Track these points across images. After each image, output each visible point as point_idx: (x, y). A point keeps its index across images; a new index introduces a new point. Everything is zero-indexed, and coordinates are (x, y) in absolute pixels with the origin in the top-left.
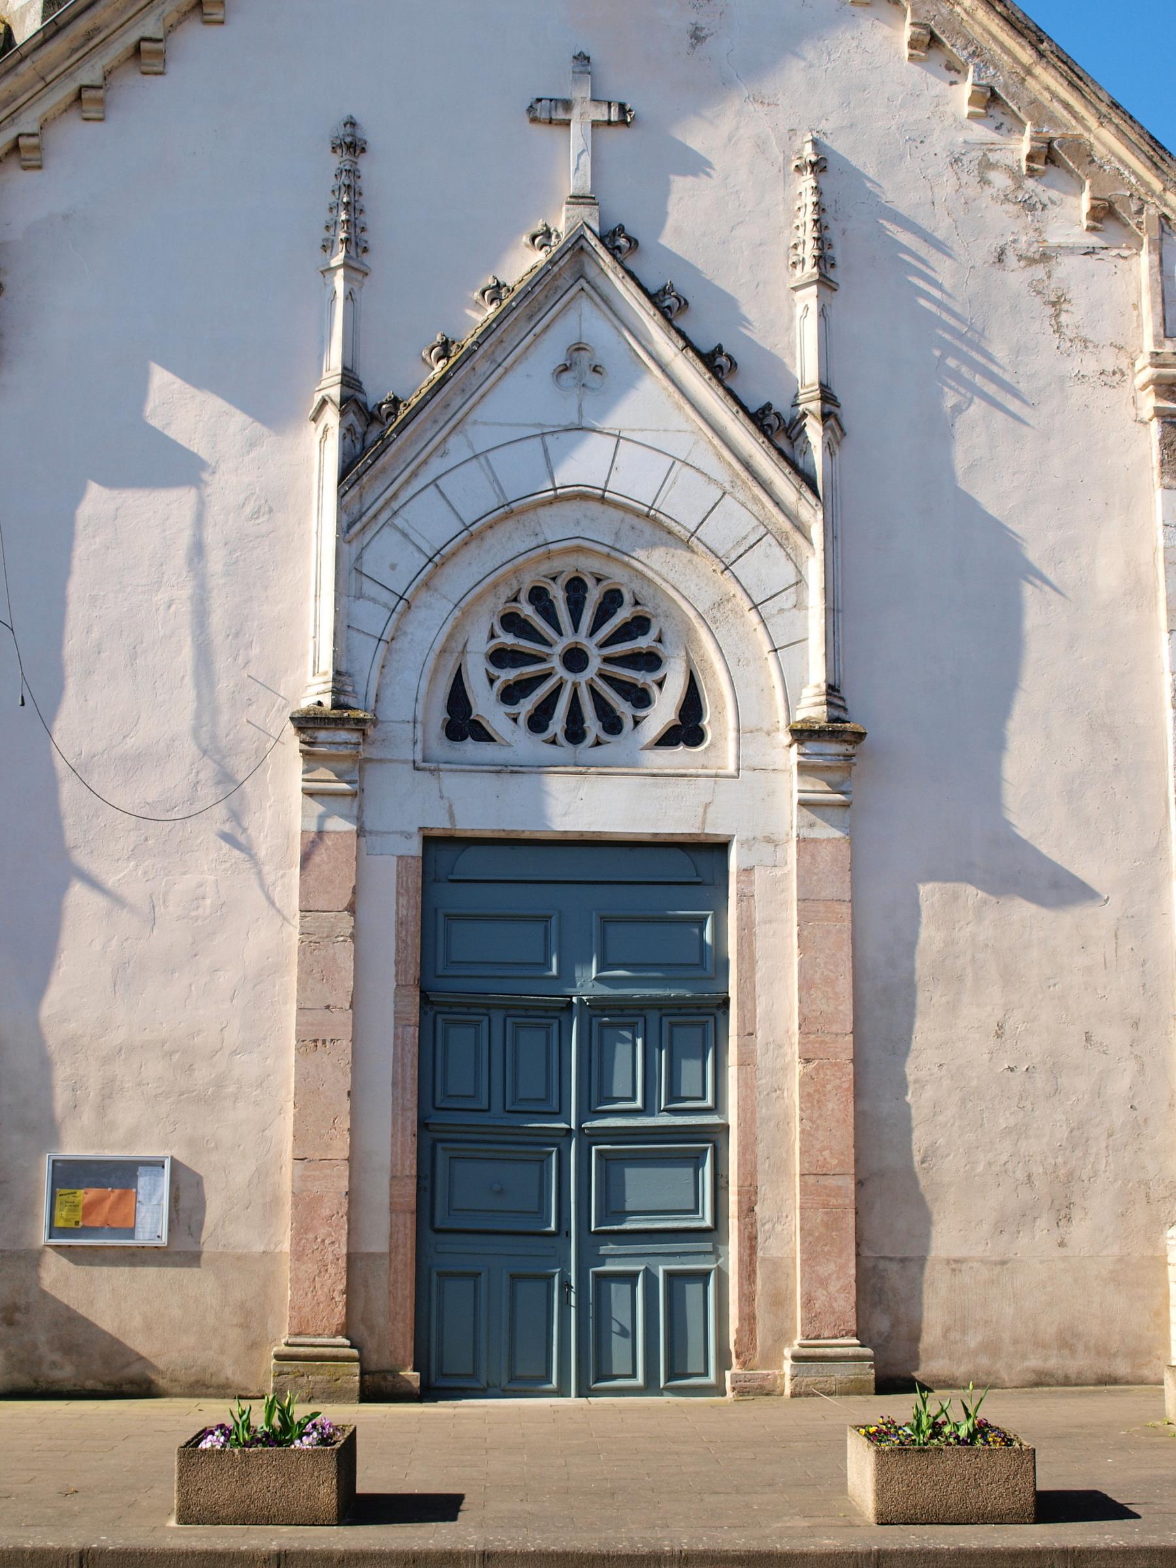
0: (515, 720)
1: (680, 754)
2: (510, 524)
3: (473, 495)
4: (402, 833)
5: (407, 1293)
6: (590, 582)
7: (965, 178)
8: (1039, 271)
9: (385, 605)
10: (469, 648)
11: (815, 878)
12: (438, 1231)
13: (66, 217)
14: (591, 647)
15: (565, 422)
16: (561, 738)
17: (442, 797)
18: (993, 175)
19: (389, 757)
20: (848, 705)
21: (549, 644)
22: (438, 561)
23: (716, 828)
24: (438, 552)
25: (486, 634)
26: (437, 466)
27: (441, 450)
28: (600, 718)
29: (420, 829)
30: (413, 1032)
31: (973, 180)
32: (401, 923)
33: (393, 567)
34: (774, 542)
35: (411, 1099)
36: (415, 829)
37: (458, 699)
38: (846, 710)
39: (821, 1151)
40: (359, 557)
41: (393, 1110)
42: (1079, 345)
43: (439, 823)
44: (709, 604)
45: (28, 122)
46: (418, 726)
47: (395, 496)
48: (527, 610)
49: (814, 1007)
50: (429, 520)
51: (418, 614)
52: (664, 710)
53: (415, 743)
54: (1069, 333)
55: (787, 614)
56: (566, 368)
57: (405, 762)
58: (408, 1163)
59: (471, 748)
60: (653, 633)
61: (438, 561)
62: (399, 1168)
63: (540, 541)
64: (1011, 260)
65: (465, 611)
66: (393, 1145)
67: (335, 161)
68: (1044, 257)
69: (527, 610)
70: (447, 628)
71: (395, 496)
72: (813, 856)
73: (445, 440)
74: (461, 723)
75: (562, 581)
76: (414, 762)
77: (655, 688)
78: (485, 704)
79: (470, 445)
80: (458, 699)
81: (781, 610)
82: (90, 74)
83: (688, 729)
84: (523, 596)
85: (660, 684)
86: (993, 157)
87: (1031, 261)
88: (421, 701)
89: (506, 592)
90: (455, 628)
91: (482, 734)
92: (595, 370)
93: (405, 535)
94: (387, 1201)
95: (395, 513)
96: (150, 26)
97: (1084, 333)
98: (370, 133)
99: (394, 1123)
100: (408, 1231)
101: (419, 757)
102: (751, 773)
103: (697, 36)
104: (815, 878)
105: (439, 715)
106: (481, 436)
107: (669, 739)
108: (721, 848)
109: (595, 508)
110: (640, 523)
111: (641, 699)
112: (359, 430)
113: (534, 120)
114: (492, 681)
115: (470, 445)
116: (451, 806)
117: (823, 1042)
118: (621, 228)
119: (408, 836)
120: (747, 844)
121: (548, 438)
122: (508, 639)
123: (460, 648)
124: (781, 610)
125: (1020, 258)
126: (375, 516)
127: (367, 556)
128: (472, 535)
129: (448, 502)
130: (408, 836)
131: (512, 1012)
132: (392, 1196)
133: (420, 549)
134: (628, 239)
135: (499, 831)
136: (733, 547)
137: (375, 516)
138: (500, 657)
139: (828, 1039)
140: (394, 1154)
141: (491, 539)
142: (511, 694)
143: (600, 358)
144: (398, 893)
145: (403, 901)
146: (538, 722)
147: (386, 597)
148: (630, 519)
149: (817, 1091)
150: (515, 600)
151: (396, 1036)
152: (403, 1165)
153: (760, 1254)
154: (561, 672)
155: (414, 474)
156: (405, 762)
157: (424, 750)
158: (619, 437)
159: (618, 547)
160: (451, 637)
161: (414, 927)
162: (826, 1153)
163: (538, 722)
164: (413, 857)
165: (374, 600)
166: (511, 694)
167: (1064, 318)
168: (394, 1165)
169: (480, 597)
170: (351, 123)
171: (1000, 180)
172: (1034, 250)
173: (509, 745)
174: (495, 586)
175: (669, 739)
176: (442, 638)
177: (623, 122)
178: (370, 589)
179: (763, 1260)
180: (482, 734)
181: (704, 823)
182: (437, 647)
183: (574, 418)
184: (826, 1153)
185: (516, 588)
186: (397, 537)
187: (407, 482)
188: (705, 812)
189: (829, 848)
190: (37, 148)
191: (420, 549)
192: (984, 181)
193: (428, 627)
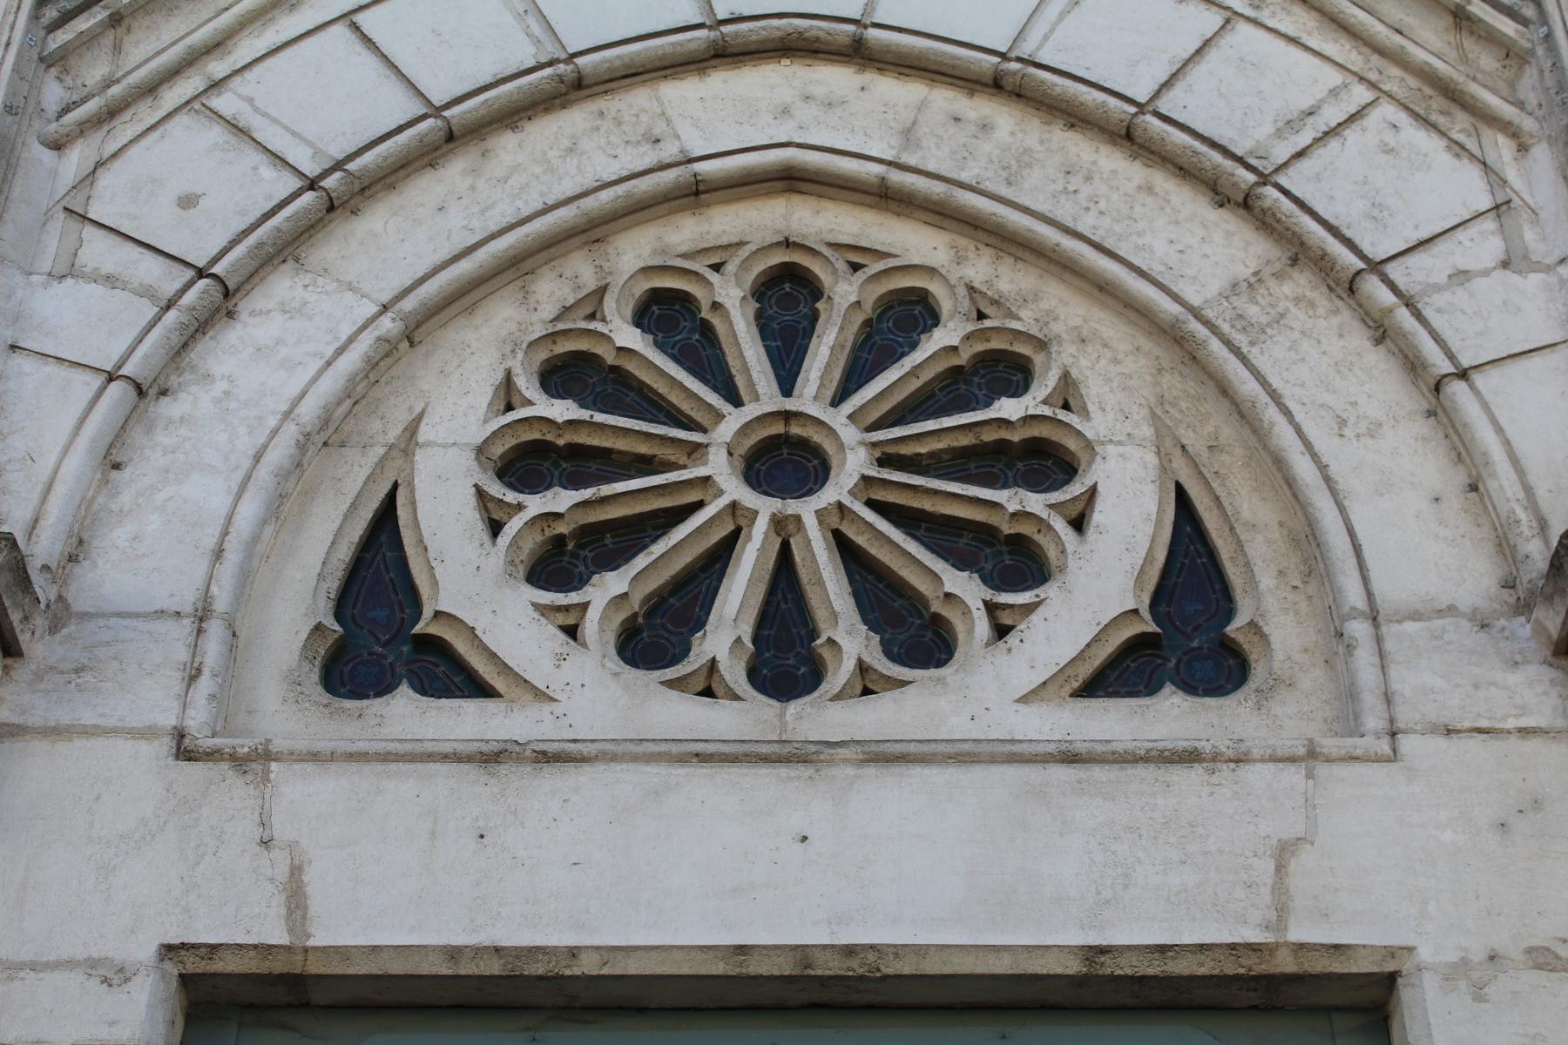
0: (572, 631)
1: (1170, 715)
9: (147, 292)
10: (425, 433)
16: (734, 673)
17: (266, 843)
19: (88, 718)
22: (340, 195)
24: (338, 166)
25: (483, 393)
29: (169, 950)
34: (1402, 118)
36: (145, 951)
44: (1214, 287)
46: (215, 629)
47: (216, 46)
52: (1102, 580)
53: (194, 676)
55: (1479, 283)
57: (147, 733)
59: (405, 714)
61: (340, 195)
63: (669, 151)
65: (420, 325)
70: (351, 361)
74: (382, 635)
76: (180, 734)
78: (469, 579)
81: (1461, 276)
85: (1079, 524)
88: (233, 557)
89: (552, 291)
91: (447, 671)
95: (216, 85)
102: (1441, 742)
105: (296, 603)
107: (1123, 671)
109: (835, 78)
111: (1017, 563)
114: (495, 528)
116: (296, 871)
120: (1477, 974)
123: (394, 433)
126: (151, 89)
127: (105, 180)
129: (384, 57)
130: (115, 975)
135: (478, 951)
136: (1279, 134)
138: (527, 462)
141: (508, 147)
142: (558, 564)
146: (655, 638)
148: (944, 99)
156: (147, 733)
159: (912, 160)
165: (111, 281)
173: (542, 696)
174: (518, 267)
175: (1123, 671)
176: (331, 384)
178: (98, 251)
180: (447, 671)
181: (1282, 910)
182: (309, 410)
185: (590, 282)
188: (1280, 868)
191: (279, 160)
193: (290, 346)
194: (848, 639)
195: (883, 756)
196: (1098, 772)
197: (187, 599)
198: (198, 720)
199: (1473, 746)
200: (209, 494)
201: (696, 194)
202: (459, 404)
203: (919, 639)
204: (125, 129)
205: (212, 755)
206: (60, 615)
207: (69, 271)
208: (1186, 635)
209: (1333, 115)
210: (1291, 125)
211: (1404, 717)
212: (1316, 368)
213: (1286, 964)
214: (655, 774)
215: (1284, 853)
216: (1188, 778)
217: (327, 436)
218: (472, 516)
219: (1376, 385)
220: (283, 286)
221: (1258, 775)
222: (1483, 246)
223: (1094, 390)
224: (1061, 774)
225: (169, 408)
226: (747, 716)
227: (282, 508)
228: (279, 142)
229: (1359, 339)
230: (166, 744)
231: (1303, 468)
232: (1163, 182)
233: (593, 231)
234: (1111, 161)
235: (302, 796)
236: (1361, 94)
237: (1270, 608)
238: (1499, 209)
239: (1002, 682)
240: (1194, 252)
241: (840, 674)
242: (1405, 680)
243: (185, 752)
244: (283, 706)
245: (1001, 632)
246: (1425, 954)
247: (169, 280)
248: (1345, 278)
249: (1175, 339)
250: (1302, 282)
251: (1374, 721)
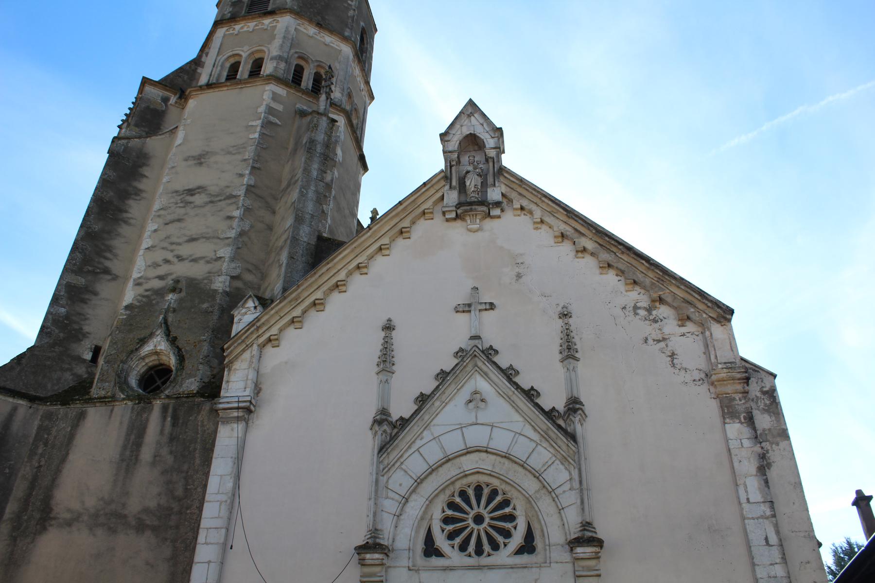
1: (525, 558)
2: (449, 464)
3: (434, 454)
6: (484, 486)
7: (627, 313)
8: (662, 344)
13: (286, 363)
14: (485, 513)
15: (470, 422)
16: (473, 554)
18: (639, 311)
20: (597, 531)
21: (467, 514)
22: (419, 481)
25: (440, 511)
26: (419, 443)
27: (420, 436)
28: (490, 544)
31: (632, 313)
33: (401, 485)
37: (429, 539)
38: (596, 533)
40: (387, 482)
42: (684, 371)
45: (274, 331)
47: (401, 456)
48: (458, 500)
50: (416, 465)
51: (411, 504)
52: (518, 539)
54: (678, 366)
56: (470, 401)
59: (435, 561)
60: (512, 506)
61: (419, 481)
63: (462, 470)
64: (650, 341)
65: (431, 501)
67: (383, 334)
68: (664, 339)
69: (458, 500)
70: (423, 509)
71: (401, 456)
73: (422, 432)
74: (431, 550)
75: (473, 487)
77: (513, 529)
78: (441, 541)
79: (432, 434)
80: (429, 539)
81: (564, 492)
82: (297, 312)
83: (528, 547)
84: (456, 494)
85: (515, 528)
86: (639, 305)
87: (659, 341)
89: (448, 492)
90: (426, 508)
91: (439, 554)
92: (482, 400)
93: (406, 472)
95: (402, 463)
96: (319, 295)
97: (684, 366)
98: (396, 322)
101: (410, 565)
103: (519, 276)
105: (420, 546)
106: (437, 431)
107: (520, 551)
109: (484, 455)
110: (504, 460)
111: (507, 534)
112: (389, 431)
113: (457, 312)
114: (443, 531)
115: (432, 434)
118: (491, 346)
121: (464, 429)
122: (450, 512)
124: (564, 492)
125: (654, 340)
126: (394, 465)
127: (390, 481)
128: (433, 470)
133: (412, 477)
134: (494, 350)
137: (394, 465)
138: (447, 520)
142: (451, 536)
143: (484, 396)
146: (463, 547)
147: (397, 497)
148: (499, 458)
150: (453, 496)
154: (472, 525)
155: (409, 447)
157: (413, 562)
158: (492, 426)
160: (425, 512)
163: (463, 547)
165: (393, 499)
166: (451, 536)
167: (675, 361)
169: (437, 495)
170: (389, 320)
171: (642, 313)
172: (660, 337)
174: (444, 490)
175: (520, 551)
177: (492, 309)
178: (391, 494)
180: (439, 554)
182: (419, 517)
183: (474, 420)
186: (403, 473)
187: (406, 450)
190: (277, 339)
191: (412, 477)
192: (636, 314)
194: (487, 547)
195: (491, 567)
196: (515, 570)
197: (407, 548)
198: (410, 565)
199: (559, 565)
200: (407, 531)
201: (466, 476)
202: (437, 513)
203: (495, 546)
204: (391, 472)
206: (393, 550)
207: (387, 498)
208: (528, 547)
209: (550, 463)
210: (544, 465)
212: (545, 505)
214: (463, 572)
216: (526, 570)
217: (422, 519)
218: (440, 531)
219: (552, 509)
220: (414, 496)
221: (534, 570)
222: (567, 487)
223: (518, 507)
224: (511, 570)
225: (402, 517)
226: (473, 561)
227: (417, 532)
228: (411, 474)
229: (551, 500)
231: (543, 522)
232: (527, 473)
233: (453, 483)
234: (520, 469)
235: (424, 575)
236: (554, 458)
237: (538, 542)
238: (570, 479)
239: (504, 556)
240: (530, 485)
241: (485, 554)
242: (553, 555)
243: (410, 570)
244: (420, 560)
245: (505, 545)
247: (400, 499)
248: (551, 492)
249: (529, 500)
250: (544, 491)
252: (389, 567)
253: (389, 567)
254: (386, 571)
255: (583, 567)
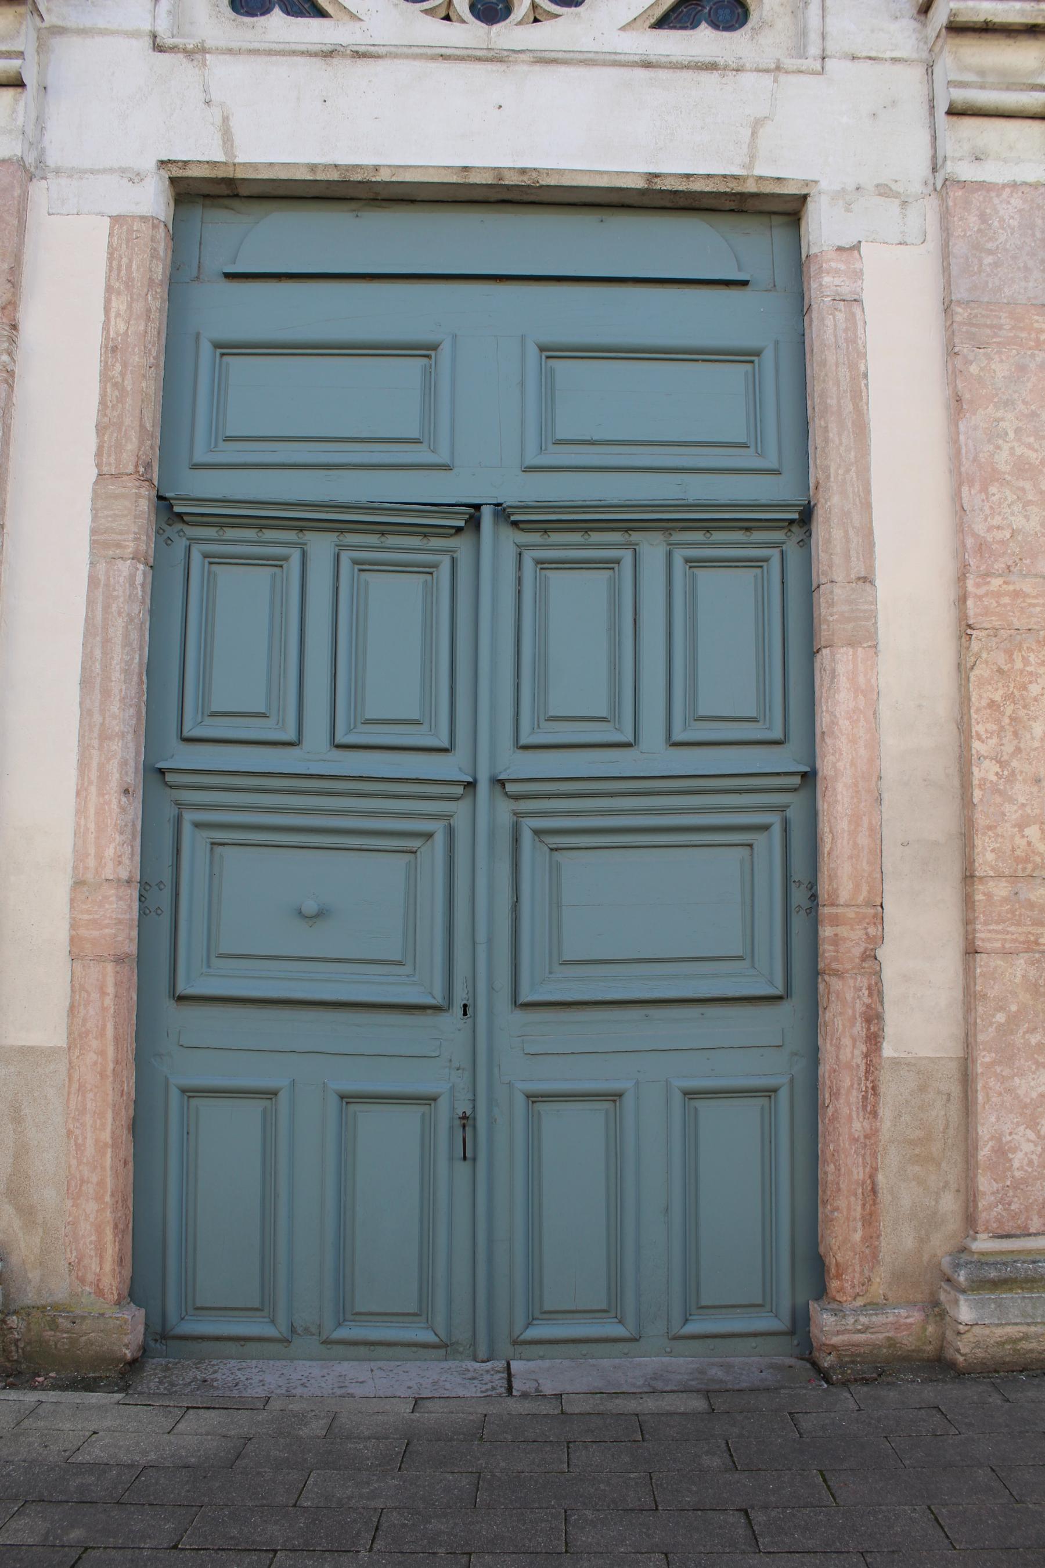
4: (123, 171)
5: (106, 1136)
11: (989, 260)
12: (181, 999)
17: (208, 103)
23: (777, 166)
30: (129, 576)
32: (112, 349)
35: (121, 714)
36: (151, 164)
39: (1021, 826)
41: (82, 737)
43: (201, 149)
49: (997, 521)
58: (110, 852)
62: (91, 862)
66: (81, 812)
72: (983, 218)
94: (63, 935)
99: (83, 766)
100: (109, 1001)
102: (849, 64)
104: (989, 260)
108: (787, 211)
116: (226, 119)
117: (1017, 594)
119: (136, 177)
120: (849, 197)
130: (136, 177)
131: (351, 538)
132: (74, 925)
135: (326, 167)
139: (1027, 586)
140: (80, 833)
144: (109, 289)
145: (119, 304)
149: (1009, 697)
151: (93, 581)
152: (100, 857)
153: (888, 1051)
161: (142, 361)
162: (1033, 832)
164: (143, 218)
168: (80, 855)
173: (354, 17)
179: (896, 1062)
181: (752, 157)
184: (1033, 832)
188: (754, 134)
189: (1016, 201)
196: (662, 74)
198: (163, 27)
205: (173, 49)
211: (831, 47)
213: (751, 187)
215: (757, 124)
221: (747, 79)
230: (147, 42)
235: (224, 72)
242: (834, 25)
243: (159, 48)
246: (824, 185)
251: (814, 50)
252: (59, 31)
253: (59, 31)
254: (42, 47)
255: (982, 73)
